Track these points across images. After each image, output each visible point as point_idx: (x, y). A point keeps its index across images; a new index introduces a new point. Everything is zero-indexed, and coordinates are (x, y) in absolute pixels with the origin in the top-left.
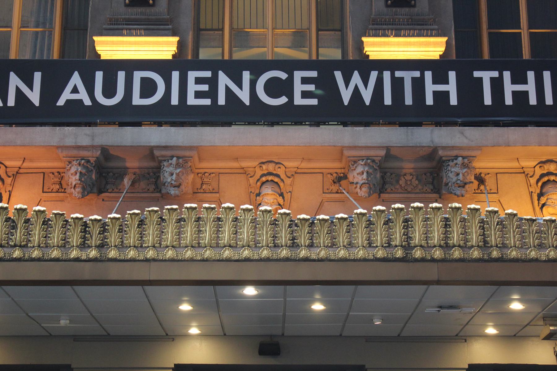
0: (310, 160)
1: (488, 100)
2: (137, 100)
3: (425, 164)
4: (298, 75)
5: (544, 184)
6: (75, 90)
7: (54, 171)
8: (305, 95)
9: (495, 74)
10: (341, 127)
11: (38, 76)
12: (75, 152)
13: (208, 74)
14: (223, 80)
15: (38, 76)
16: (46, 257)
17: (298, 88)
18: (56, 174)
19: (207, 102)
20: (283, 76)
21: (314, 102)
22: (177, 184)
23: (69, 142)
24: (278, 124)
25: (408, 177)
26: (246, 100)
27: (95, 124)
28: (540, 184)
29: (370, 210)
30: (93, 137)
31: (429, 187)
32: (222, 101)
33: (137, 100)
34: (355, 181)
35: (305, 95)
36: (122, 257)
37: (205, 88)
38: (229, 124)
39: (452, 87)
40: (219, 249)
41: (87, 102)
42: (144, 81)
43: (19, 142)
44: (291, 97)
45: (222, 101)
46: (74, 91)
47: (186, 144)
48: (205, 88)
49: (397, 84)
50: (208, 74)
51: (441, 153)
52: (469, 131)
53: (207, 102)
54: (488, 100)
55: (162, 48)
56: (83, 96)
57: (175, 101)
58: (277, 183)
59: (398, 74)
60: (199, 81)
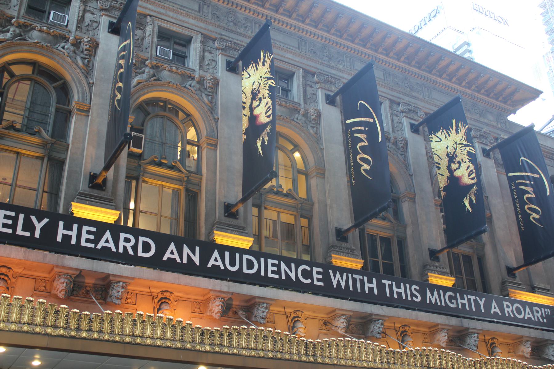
0: (314, 312)
1: (388, 295)
2: (245, 271)
3: (360, 321)
4: (315, 269)
5: (295, 321)
6: (107, 241)
7: (42, 278)
8: (318, 280)
9: (390, 282)
10: (274, 289)
11: (197, 249)
12: (219, 294)
13: (276, 262)
14: (284, 267)
15: (197, 249)
16: (183, 348)
17: (316, 276)
18: (43, 281)
19: (277, 276)
20: (309, 269)
21: (322, 284)
22: (120, 297)
23: (218, 288)
24: (307, 293)
25: (353, 326)
26: (294, 279)
27: (226, 280)
28: (160, 303)
29: (231, 327)
30: (229, 287)
31: (360, 332)
32: (283, 277)
33: (245, 271)
34: (338, 326)
35: (318, 280)
36: (78, 336)
37: (275, 269)
38: (265, 286)
39: (374, 286)
40: (134, 338)
41: (222, 267)
42: (249, 261)
43: (193, 285)
44: (312, 280)
45: (283, 277)
46: (215, 260)
47: (272, 297)
48: (275, 269)
49: (354, 280)
50: (276, 262)
51: (373, 317)
52: (385, 308)
53: (277, 276)
54: (388, 295)
55: (244, 242)
56: (219, 263)
57: (263, 274)
58: (6, 280)
59: (354, 276)
60: (273, 265)
